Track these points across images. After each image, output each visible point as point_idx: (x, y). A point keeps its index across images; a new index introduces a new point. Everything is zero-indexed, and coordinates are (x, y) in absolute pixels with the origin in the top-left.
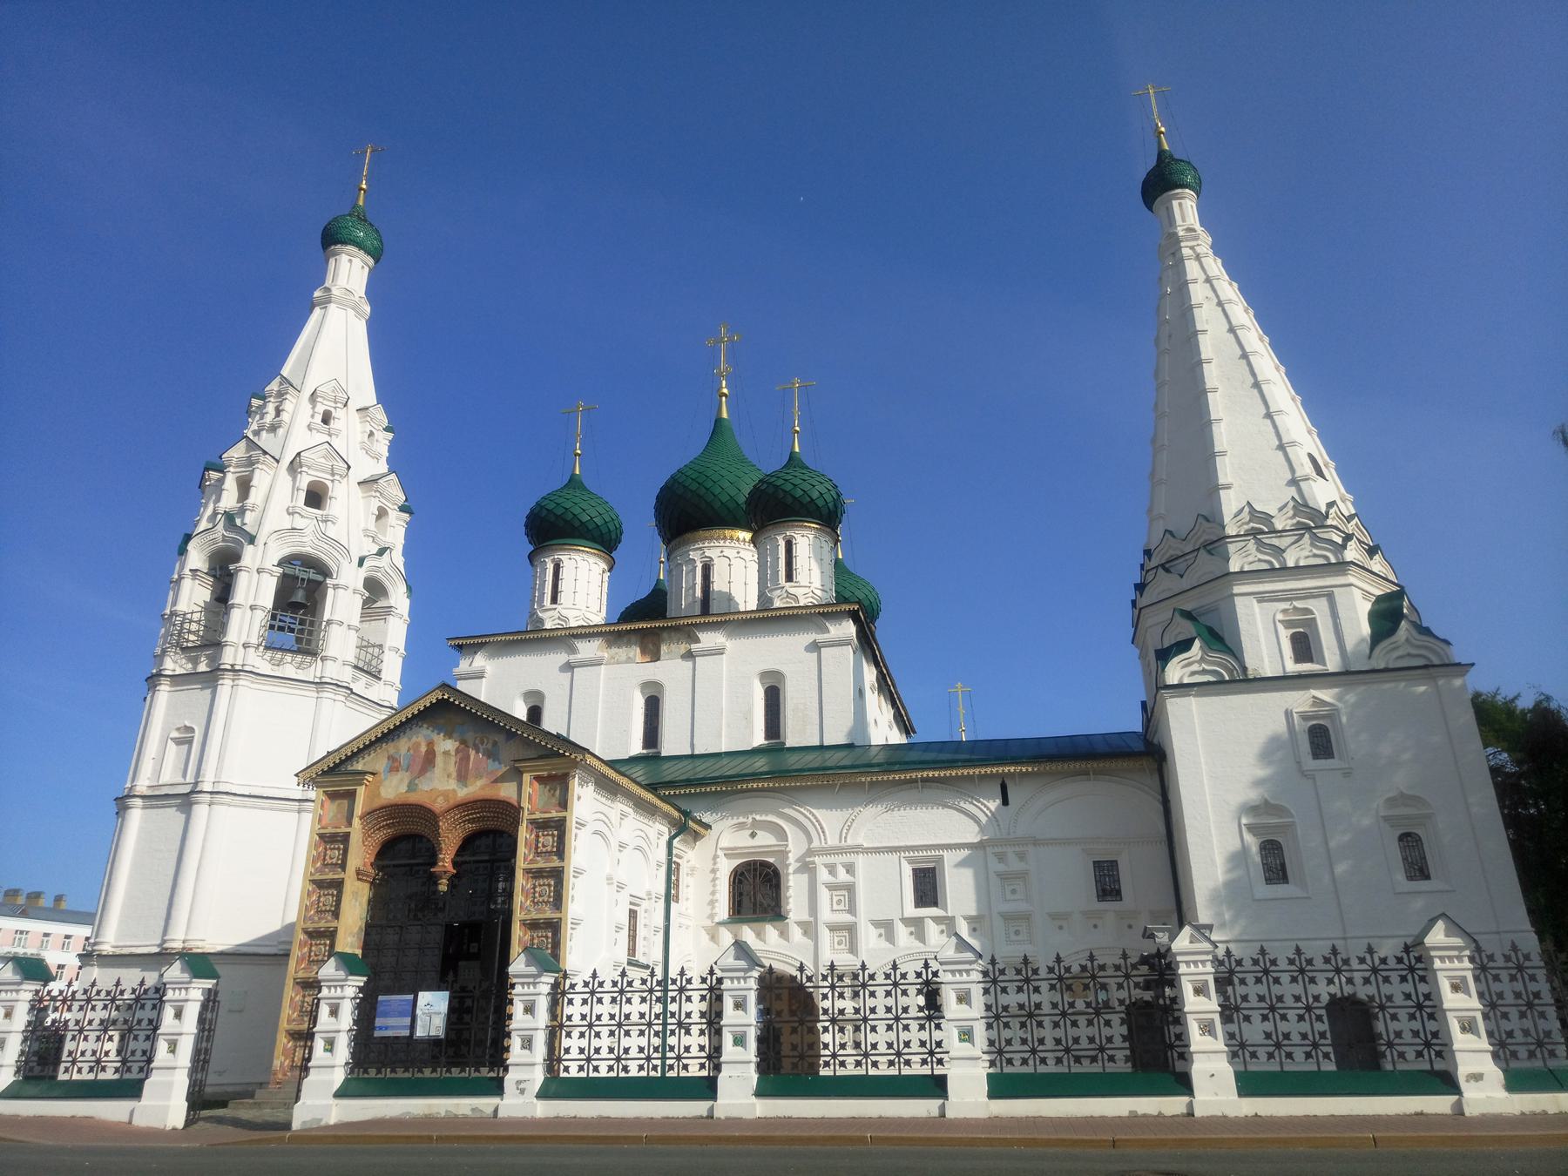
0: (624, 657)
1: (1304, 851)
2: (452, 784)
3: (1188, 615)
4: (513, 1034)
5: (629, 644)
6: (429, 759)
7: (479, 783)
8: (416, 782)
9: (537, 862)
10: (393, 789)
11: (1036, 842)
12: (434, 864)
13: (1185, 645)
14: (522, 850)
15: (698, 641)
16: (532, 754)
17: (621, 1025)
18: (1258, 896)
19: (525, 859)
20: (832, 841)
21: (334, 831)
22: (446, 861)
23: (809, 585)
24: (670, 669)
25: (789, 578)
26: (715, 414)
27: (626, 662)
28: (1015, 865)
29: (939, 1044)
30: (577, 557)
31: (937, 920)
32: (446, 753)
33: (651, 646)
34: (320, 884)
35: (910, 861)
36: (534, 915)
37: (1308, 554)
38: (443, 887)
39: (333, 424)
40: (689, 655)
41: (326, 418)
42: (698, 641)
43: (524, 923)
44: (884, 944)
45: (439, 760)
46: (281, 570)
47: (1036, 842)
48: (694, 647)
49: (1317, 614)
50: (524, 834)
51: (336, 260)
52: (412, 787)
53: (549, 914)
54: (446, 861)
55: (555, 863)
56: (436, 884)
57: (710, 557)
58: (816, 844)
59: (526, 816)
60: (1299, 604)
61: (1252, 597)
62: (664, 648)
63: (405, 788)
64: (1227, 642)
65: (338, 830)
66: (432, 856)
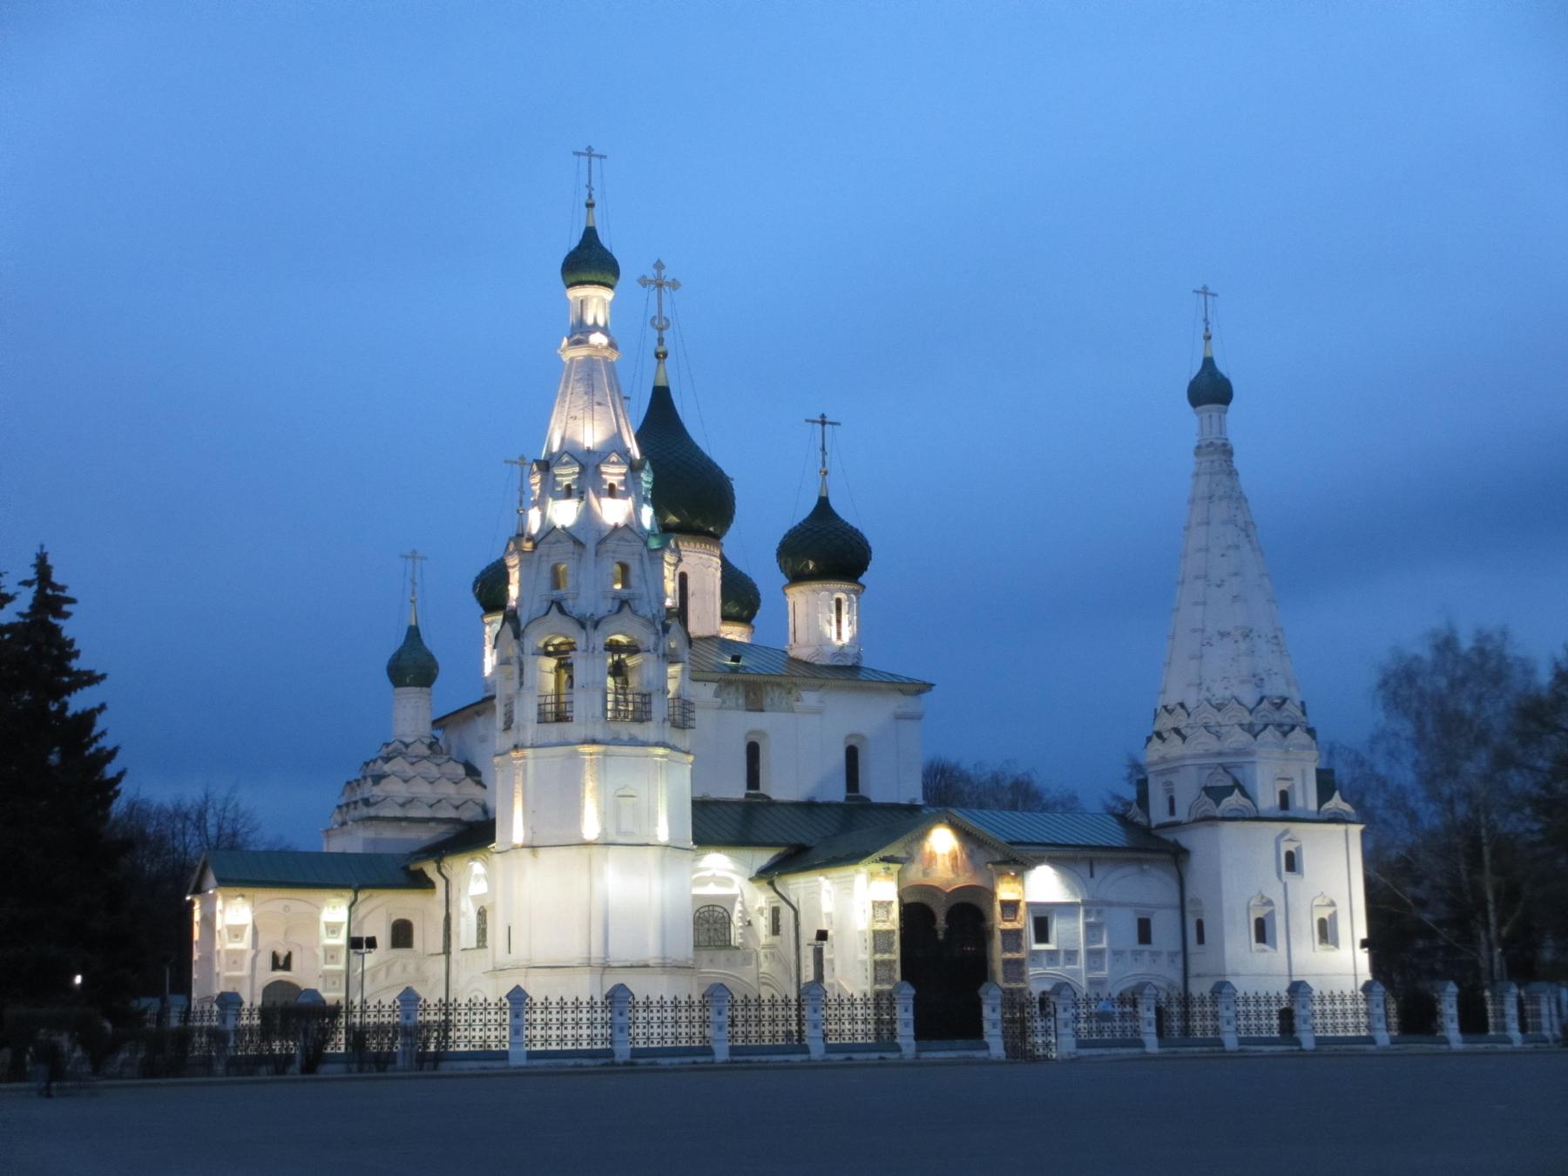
3: (1226, 769)
4: (898, 1022)
11: (1110, 904)
13: (1228, 791)
17: (546, 1025)
22: (941, 922)
26: (653, 380)
31: (1049, 952)
32: (944, 855)
33: (751, 694)
38: (941, 936)
40: (791, 710)
47: (1110, 904)
54: (941, 922)
62: (769, 700)
64: (1248, 789)
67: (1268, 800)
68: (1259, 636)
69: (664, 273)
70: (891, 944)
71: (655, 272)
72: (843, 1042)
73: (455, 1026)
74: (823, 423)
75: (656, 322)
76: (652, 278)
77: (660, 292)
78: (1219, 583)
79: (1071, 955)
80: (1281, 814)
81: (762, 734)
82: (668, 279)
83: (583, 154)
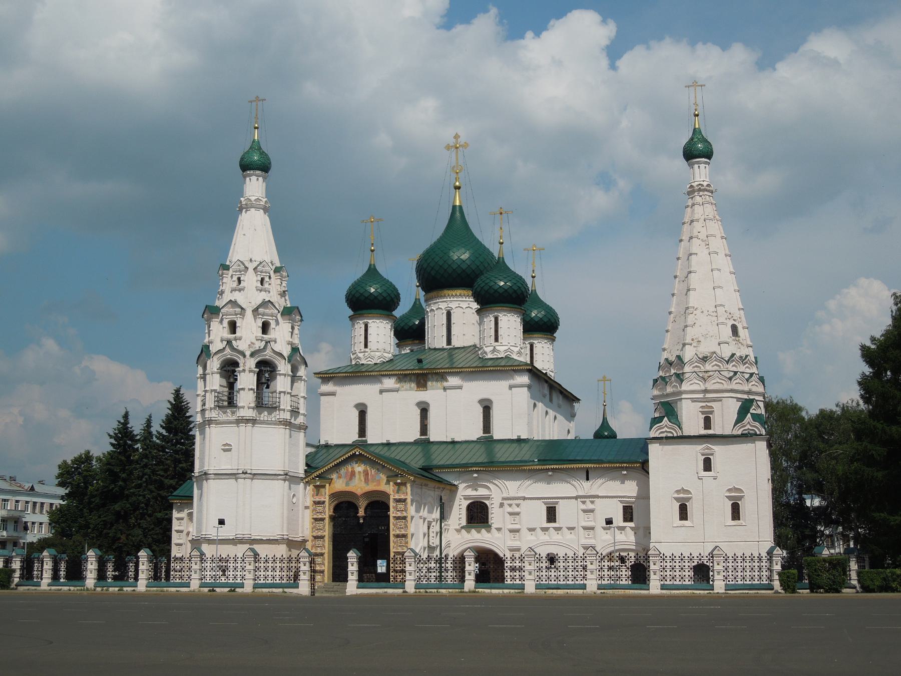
0: (409, 388)
1: (693, 509)
2: (363, 484)
5: (411, 381)
6: (353, 474)
7: (375, 483)
8: (349, 482)
9: (397, 514)
10: (339, 484)
11: (598, 497)
12: (358, 513)
14: (391, 509)
15: (447, 381)
16: (393, 474)
18: (675, 525)
19: (393, 513)
20: (512, 494)
21: (319, 500)
22: (361, 513)
23: (507, 344)
24: (433, 394)
25: (496, 340)
27: (410, 390)
28: (590, 506)
29: (524, 576)
30: (378, 321)
31: (554, 528)
32: (359, 472)
33: (422, 381)
34: (316, 520)
35: (545, 503)
36: (398, 532)
37: (715, 381)
39: (266, 286)
40: (445, 389)
41: (262, 281)
42: (447, 381)
43: (394, 535)
44: (533, 538)
45: (357, 475)
46: (258, 370)
48: (445, 384)
49: (715, 409)
50: (392, 504)
51: (250, 179)
52: (347, 484)
53: (403, 532)
54: (361, 513)
55: (405, 514)
56: (359, 520)
57: (451, 308)
58: (505, 495)
59: (392, 497)
60: (709, 404)
61: (689, 400)
62: (429, 383)
63: (344, 485)
65: (321, 500)
66: (356, 508)
67: (692, 423)
68: (702, 312)
69: (459, 140)
70: (324, 526)
71: (454, 140)
72: (275, 582)
73: (628, 568)
74: (501, 214)
75: (455, 169)
76: (454, 145)
77: (457, 152)
78: (683, 279)
79: (571, 529)
80: (704, 432)
81: (427, 404)
82: (462, 143)
83: (254, 101)
